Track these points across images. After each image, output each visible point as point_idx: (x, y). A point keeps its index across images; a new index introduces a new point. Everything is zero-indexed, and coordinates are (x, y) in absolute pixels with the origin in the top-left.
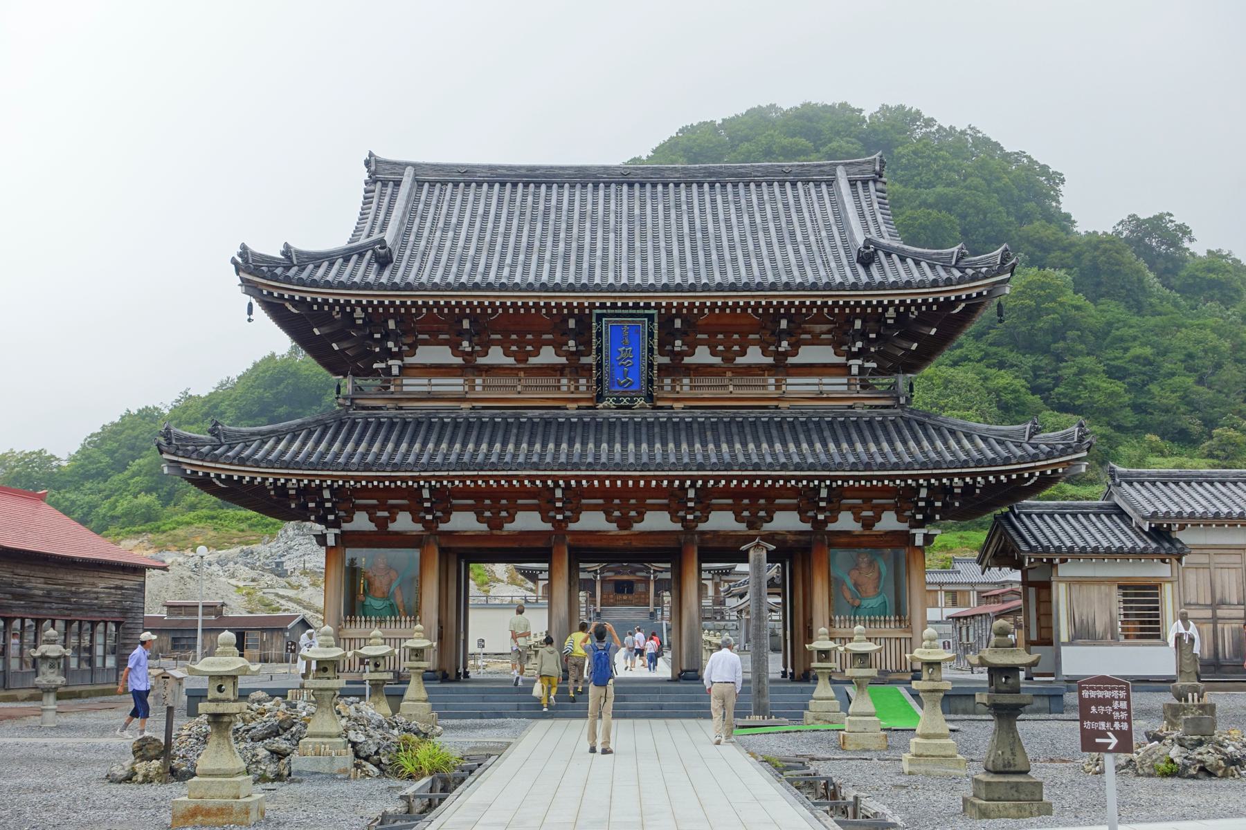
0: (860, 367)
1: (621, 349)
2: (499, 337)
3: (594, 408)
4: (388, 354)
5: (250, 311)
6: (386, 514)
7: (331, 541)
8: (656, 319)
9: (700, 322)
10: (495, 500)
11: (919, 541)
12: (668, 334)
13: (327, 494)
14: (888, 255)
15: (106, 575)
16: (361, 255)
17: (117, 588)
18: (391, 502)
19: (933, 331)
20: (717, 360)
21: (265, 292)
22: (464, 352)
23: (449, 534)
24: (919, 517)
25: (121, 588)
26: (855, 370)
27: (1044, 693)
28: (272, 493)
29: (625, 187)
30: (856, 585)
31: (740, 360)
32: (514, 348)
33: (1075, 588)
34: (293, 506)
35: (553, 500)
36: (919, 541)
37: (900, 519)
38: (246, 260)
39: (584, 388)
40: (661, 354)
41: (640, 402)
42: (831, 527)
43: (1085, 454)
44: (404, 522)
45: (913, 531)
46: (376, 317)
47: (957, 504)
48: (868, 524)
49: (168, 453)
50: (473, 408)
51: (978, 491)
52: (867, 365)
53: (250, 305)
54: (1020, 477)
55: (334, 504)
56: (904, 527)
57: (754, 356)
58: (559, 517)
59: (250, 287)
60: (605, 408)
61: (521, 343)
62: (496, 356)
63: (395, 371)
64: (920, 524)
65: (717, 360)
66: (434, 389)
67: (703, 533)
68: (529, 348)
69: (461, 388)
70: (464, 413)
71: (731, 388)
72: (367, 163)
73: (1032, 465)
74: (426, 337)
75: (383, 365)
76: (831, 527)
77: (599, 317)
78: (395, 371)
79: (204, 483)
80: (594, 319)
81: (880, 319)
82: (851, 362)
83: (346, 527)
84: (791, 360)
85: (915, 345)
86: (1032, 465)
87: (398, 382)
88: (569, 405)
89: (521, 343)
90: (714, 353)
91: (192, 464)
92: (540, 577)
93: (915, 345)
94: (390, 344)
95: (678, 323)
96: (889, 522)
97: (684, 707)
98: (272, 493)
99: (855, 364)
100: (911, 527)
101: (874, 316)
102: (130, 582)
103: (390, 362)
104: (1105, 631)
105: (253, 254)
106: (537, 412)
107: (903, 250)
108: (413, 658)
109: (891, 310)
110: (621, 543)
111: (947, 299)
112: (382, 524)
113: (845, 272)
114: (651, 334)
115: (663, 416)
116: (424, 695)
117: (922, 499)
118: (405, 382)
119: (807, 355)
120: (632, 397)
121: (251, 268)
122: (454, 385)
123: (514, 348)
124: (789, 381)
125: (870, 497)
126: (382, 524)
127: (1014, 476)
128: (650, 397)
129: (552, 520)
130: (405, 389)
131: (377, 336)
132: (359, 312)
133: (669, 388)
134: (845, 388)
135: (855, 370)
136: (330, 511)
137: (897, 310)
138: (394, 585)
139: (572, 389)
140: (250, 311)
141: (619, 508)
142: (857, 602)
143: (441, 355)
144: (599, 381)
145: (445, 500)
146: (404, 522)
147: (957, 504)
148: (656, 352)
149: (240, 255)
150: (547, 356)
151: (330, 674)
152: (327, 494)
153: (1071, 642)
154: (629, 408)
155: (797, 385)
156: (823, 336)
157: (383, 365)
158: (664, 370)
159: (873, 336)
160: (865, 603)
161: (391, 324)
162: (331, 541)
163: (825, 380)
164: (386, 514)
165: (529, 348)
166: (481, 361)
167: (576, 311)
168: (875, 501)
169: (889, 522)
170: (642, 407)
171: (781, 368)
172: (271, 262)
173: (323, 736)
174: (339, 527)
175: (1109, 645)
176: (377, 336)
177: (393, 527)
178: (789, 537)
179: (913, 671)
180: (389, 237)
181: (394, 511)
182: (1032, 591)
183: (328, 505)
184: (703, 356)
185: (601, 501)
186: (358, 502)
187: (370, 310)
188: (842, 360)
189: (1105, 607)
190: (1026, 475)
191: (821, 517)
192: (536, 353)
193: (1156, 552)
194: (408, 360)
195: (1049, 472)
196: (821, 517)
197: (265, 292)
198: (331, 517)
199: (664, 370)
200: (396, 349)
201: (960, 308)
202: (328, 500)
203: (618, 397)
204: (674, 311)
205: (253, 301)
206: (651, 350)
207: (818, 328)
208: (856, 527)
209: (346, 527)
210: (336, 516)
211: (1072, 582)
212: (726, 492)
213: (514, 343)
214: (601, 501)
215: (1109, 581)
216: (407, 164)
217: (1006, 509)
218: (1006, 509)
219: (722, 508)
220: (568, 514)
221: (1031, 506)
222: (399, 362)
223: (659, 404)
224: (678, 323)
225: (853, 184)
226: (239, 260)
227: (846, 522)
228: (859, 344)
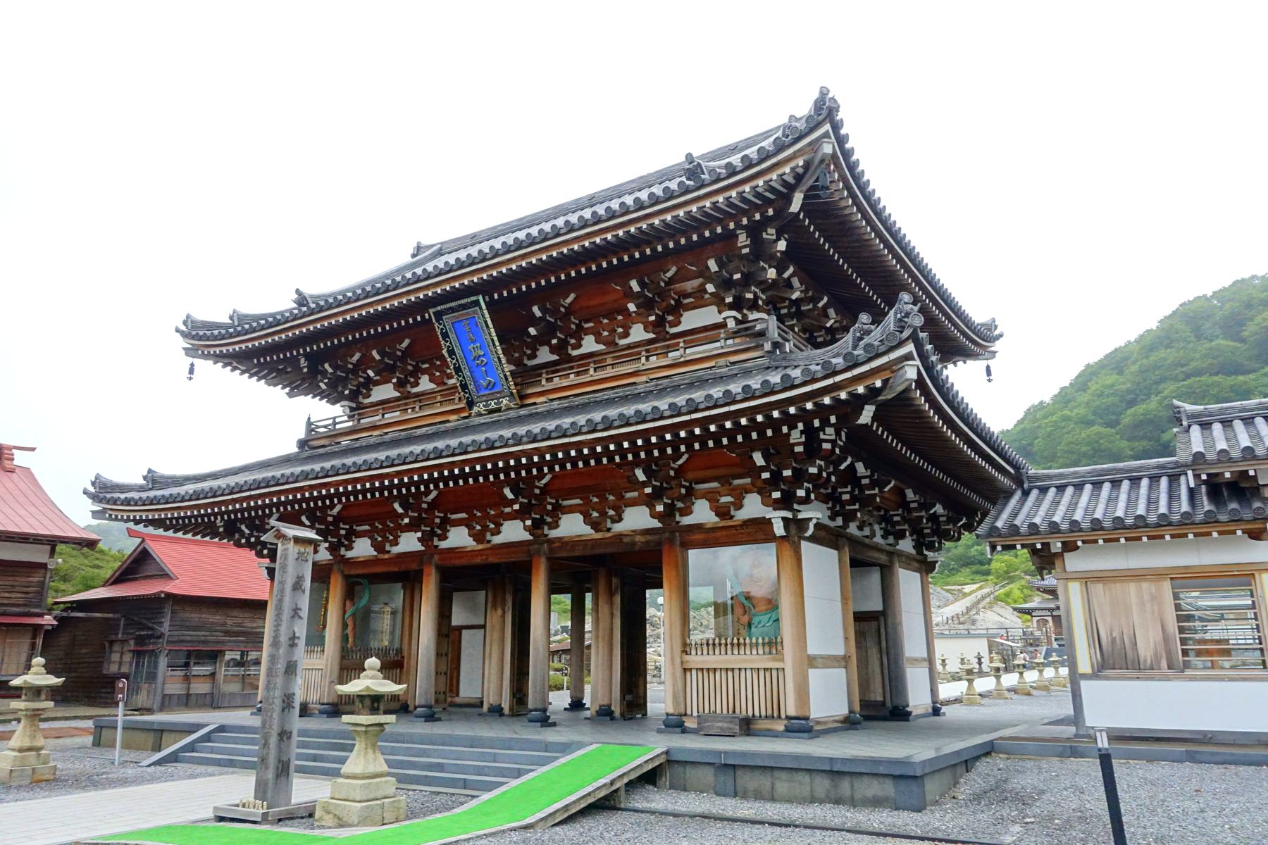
33: (1098, 589)
48: (723, 513)
60: (479, 414)
67: (551, 541)
104: (1157, 657)
110: (478, 560)
144: (464, 387)
153: (1096, 675)
154: (499, 410)
171: (662, 337)
175: (1166, 678)
178: (638, 538)
189: (1146, 619)
191: (660, 508)
193: (1210, 520)
211: (1088, 579)
215: (1157, 575)
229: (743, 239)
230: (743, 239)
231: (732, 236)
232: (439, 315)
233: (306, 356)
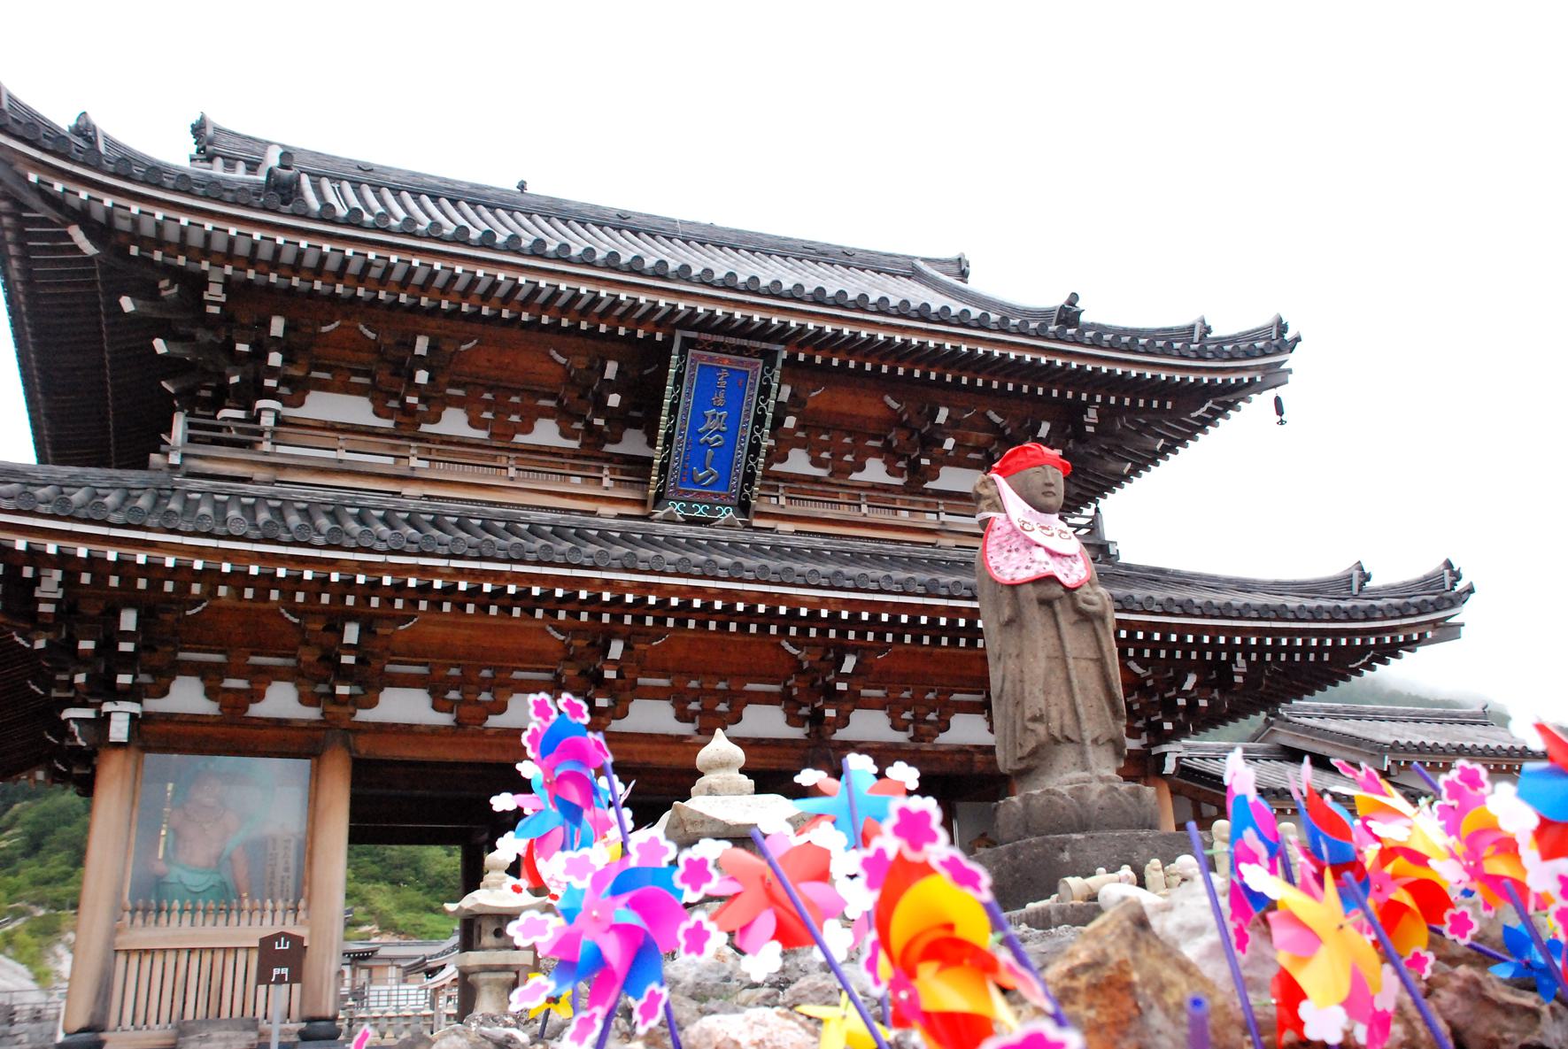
2: (460, 392)
3: (646, 518)
6: (241, 684)
23: (382, 728)
40: (771, 437)
41: (726, 514)
45: (1165, 748)
57: (875, 471)
60: (669, 520)
65: (821, 472)
68: (515, 418)
70: (412, 505)
80: (676, 349)
83: (154, 705)
88: (604, 509)
90: (816, 462)
103: (260, 404)
106: (547, 516)
120: (713, 505)
123: (487, 415)
126: (235, 705)
128: (744, 507)
136: (127, 662)
150: (546, 433)
154: (706, 522)
164: (241, 684)
165: (515, 418)
170: (729, 525)
176: (243, 347)
177: (257, 710)
185: (664, 682)
186: (183, 656)
192: (527, 428)
198: (124, 679)
209: (154, 705)
213: (488, 406)
214: (664, 682)
219: (869, 704)
223: (757, 523)
229: (1092, 415)
230: (1092, 415)
231: (1085, 406)
232: (688, 344)
233: (228, 284)
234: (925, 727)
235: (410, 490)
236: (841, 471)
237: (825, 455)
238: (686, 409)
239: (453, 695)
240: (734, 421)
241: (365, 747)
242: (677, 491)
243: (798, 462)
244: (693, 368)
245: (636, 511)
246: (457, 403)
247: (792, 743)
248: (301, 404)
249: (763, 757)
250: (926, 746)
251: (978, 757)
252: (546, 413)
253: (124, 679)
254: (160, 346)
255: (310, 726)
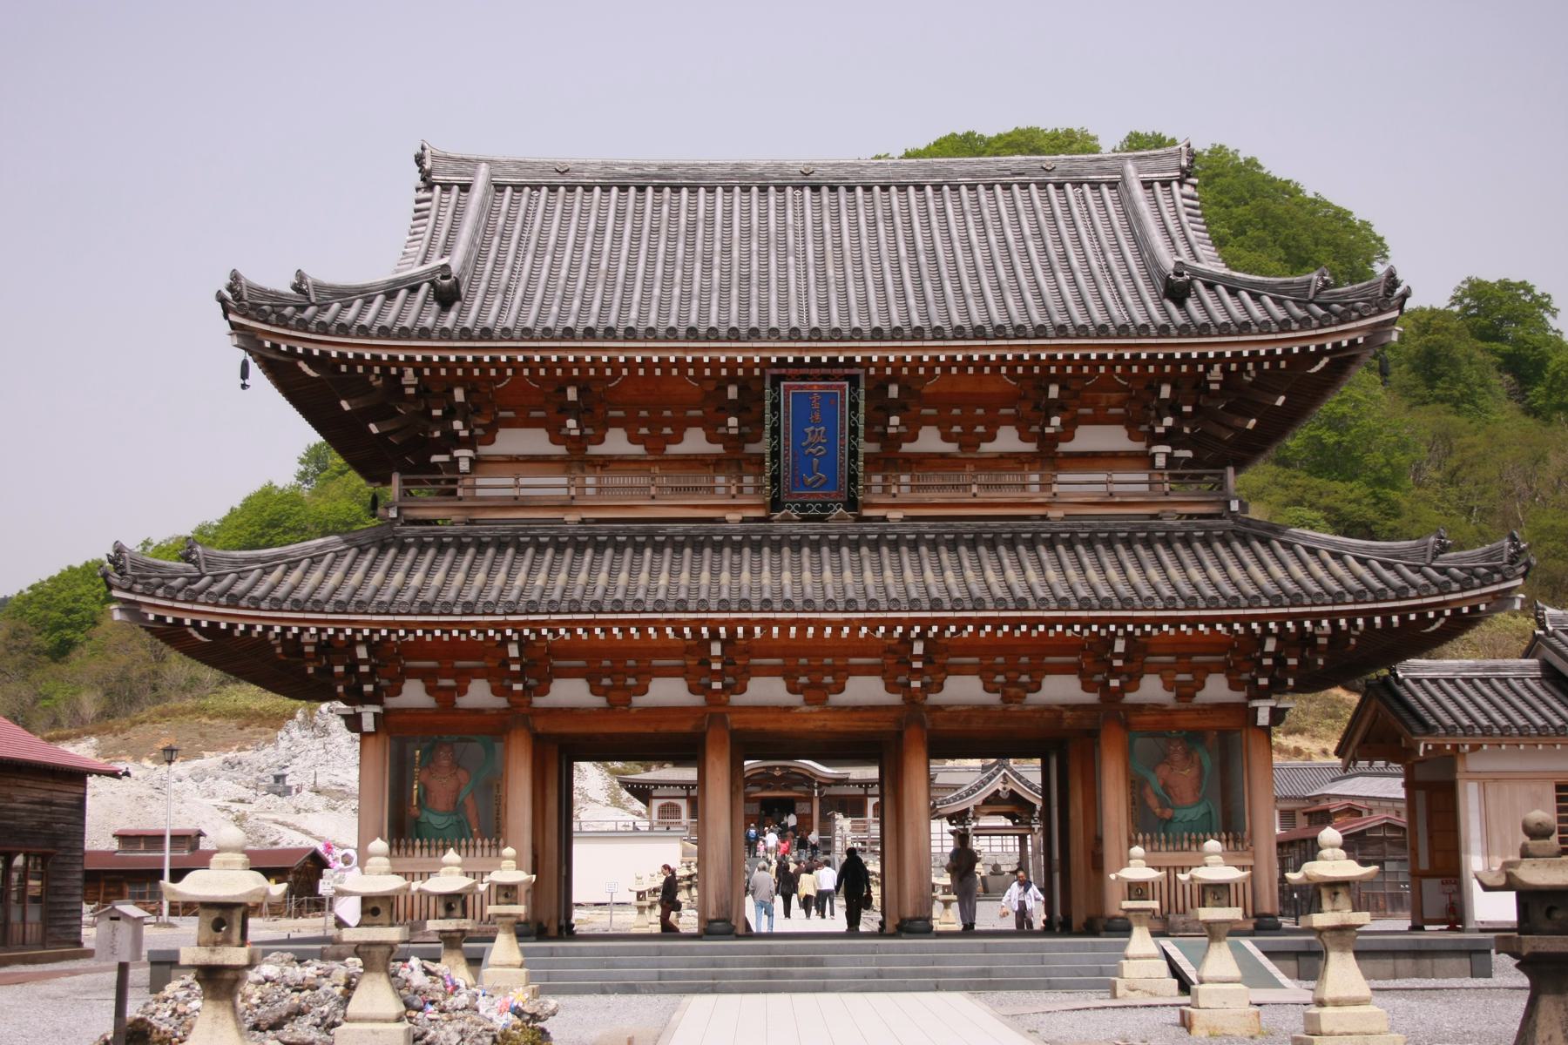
0: (1169, 456)
1: (809, 430)
2: (620, 413)
4: (452, 441)
5: (245, 373)
7: (368, 724)
8: (862, 384)
9: (926, 390)
10: (618, 663)
11: (1263, 718)
12: (880, 408)
13: (362, 653)
14: (1210, 286)
15: (28, 783)
16: (414, 290)
17: (43, 803)
18: (459, 664)
19: (1280, 401)
20: (951, 448)
21: (267, 344)
22: (569, 436)
24: (1263, 681)
25: (50, 804)
26: (1160, 461)
27: (1463, 947)
28: (279, 650)
29: (807, 192)
30: (1166, 787)
31: (986, 447)
32: (644, 431)
33: (1490, 788)
34: (310, 670)
35: (705, 662)
36: (1263, 718)
37: (1234, 686)
38: (238, 296)
39: (751, 490)
40: (868, 439)
42: (1130, 698)
43: (1519, 582)
44: (479, 694)
45: (1255, 703)
46: (435, 382)
47: (1321, 662)
48: (1185, 693)
49: (120, 589)
50: (583, 521)
51: (1353, 641)
52: (1180, 453)
53: (245, 365)
54: (1422, 617)
55: (373, 667)
56: (1238, 697)
57: (1008, 440)
58: (717, 685)
59: (247, 339)
61: (655, 423)
62: (616, 443)
63: (464, 466)
64: (1264, 694)
65: (951, 448)
66: (524, 492)
67: (938, 708)
68: (667, 431)
69: (564, 491)
71: (975, 489)
72: (419, 160)
73: (1440, 599)
74: (511, 414)
75: (445, 458)
76: (1130, 698)
77: (776, 381)
78: (464, 466)
79: (172, 635)
81: (1200, 382)
82: (1155, 449)
83: (392, 702)
84: (1064, 447)
85: (1253, 422)
86: (1440, 599)
87: (468, 482)
88: (730, 516)
89: (655, 423)
90: (946, 437)
91: (155, 606)
92: (655, 793)
93: (1253, 422)
94: (457, 425)
95: (894, 391)
96: (1216, 689)
97: (917, 974)
98: (279, 650)
99: (1161, 450)
100: (1251, 697)
101: (1189, 377)
102: (64, 795)
103: (457, 453)
105: (250, 288)
106: (681, 527)
107: (1234, 279)
108: (502, 899)
109: (1217, 367)
111: (1304, 350)
112: (445, 698)
113: (1149, 308)
114: (854, 406)
115: (872, 531)
116: (518, 958)
117: (1269, 655)
118: (479, 482)
119: (1089, 438)
120: (825, 504)
121: (245, 307)
122: (553, 485)
123: (644, 431)
124: (1061, 477)
125: (1188, 655)
126: (445, 698)
127: (1413, 617)
128: (852, 504)
129: (705, 689)
130: (479, 492)
131: (437, 413)
132: (409, 376)
133: (879, 489)
134: (1145, 488)
135: (1160, 461)
136: (368, 678)
137: (1225, 370)
138: (465, 791)
139: (734, 491)
140: (245, 373)
141: (807, 670)
142: (1168, 813)
143: (535, 441)
145: (543, 662)
146: (479, 694)
147: (1321, 662)
148: (861, 434)
149: (230, 288)
150: (695, 442)
151: (384, 916)
152: (362, 653)
154: (821, 519)
155: (1075, 485)
156: (1112, 411)
157: (445, 458)
158: (873, 463)
159: (1187, 409)
160: (1179, 814)
161: (459, 395)
162: (368, 724)
163: (1116, 477)
165: (667, 431)
166: (594, 450)
167: (740, 372)
168: (1196, 659)
169: (1216, 689)
170: (840, 518)
171: (1049, 457)
172: (278, 299)
173: (373, 1020)
174: (381, 703)
176: (437, 413)
177: (464, 702)
179: (1255, 916)
180: (455, 261)
181: (464, 677)
182: (1421, 796)
183: (364, 669)
184: (930, 441)
187: (427, 372)
188: (1139, 446)
190: (1431, 615)
191: (1114, 683)
192: (678, 439)
194: (484, 450)
195: (1465, 610)
196: (1114, 683)
197: (267, 344)
198: (368, 688)
199: (873, 463)
200: (464, 433)
201: (1322, 364)
202: (364, 662)
203: (803, 504)
204: (889, 371)
205: (250, 359)
206: (854, 431)
207: (1104, 398)
208: (1166, 697)
209: (392, 702)
210: (376, 685)
212: (968, 648)
213: (644, 422)
216: (479, 161)
217: (1385, 672)
218: (1385, 672)
219: (960, 670)
220: (729, 680)
221: (1422, 668)
222: (469, 453)
223: (867, 513)
224: (894, 391)
225: (1148, 185)
226: (228, 295)
227: (1151, 689)
228: (1168, 421)
234: (1013, 691)
235: (572, 517)
236: (969, 442)
237: (957, 429)
238: (786, 428)
239: (606, 682)
240: (831, 435)
241: (541, 725)
242: (790, 495)
243: (930, 441)
244: (787, 397)
245: (760, 513)
246: (617, 423)
247: (888, 708)
248: (492, 441)
249: (862, 720)
250: (1014, 707)
251: (1068, 714)
252: (695, 423)
253: (368, 688)
254: (374, 428)
255: (500, 712)
